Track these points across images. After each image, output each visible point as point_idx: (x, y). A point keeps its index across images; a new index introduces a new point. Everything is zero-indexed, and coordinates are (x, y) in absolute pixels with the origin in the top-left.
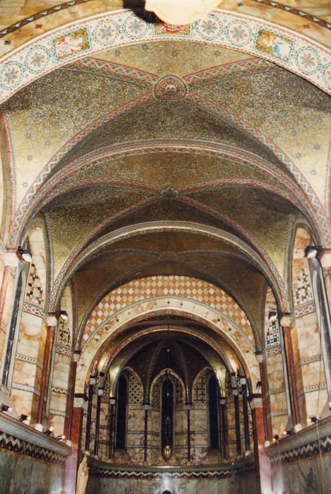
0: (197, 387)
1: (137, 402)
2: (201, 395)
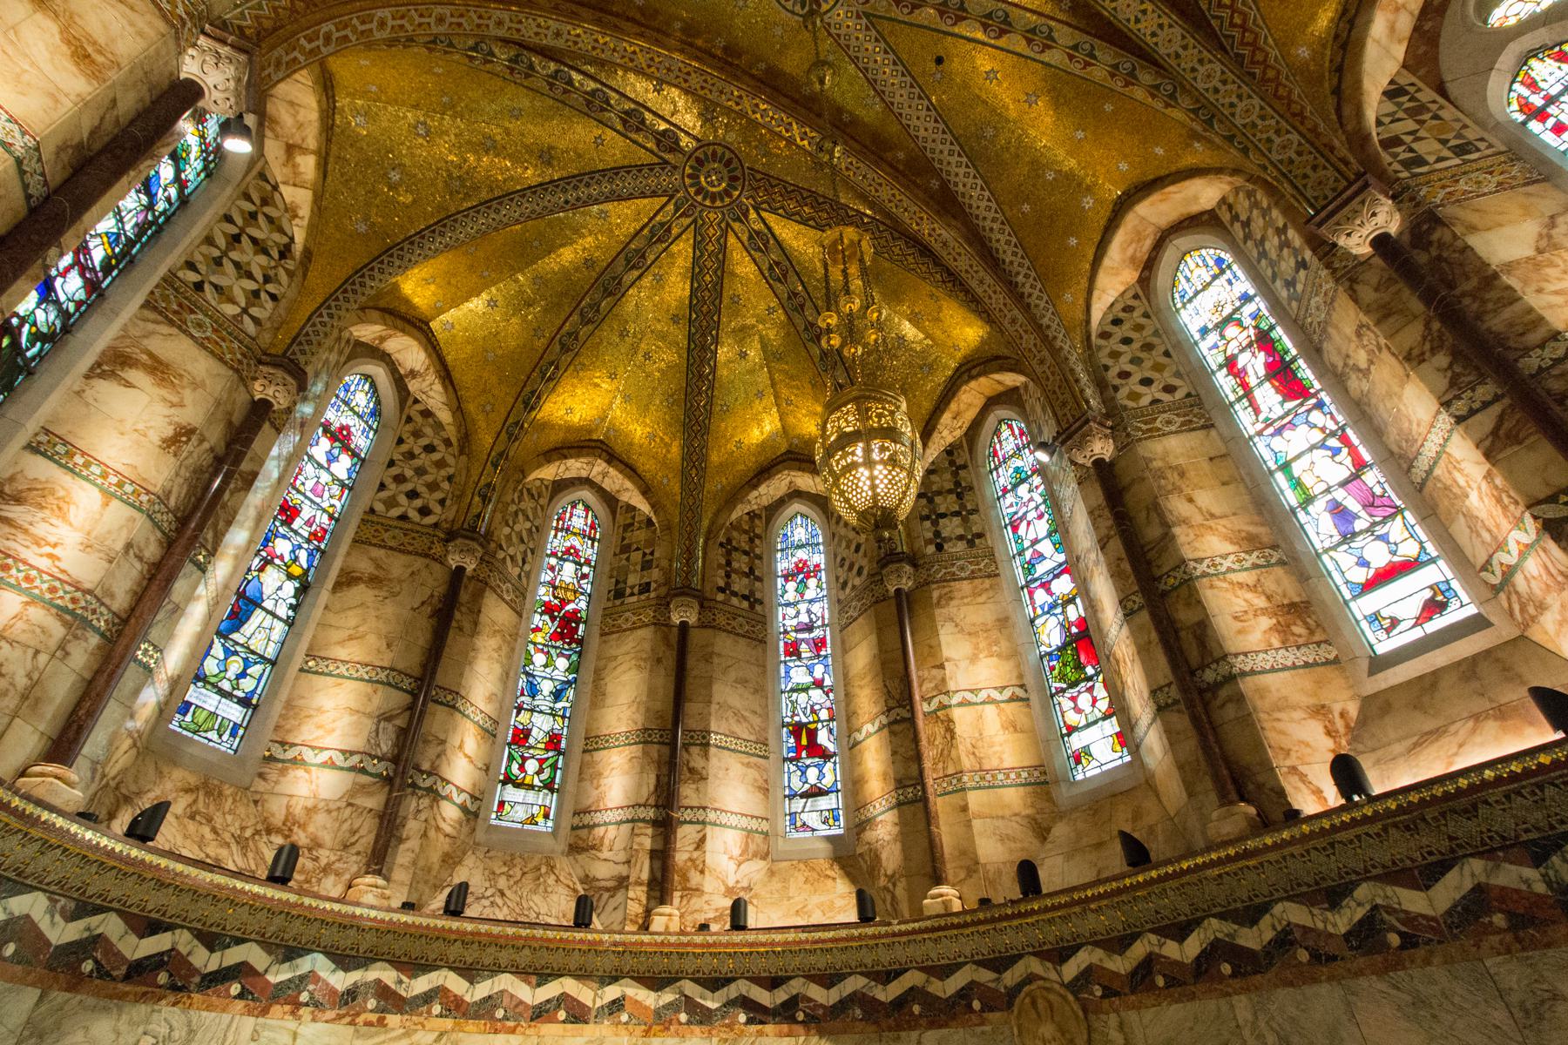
0: (729, 541)
1: (413, 515)
2: (747, 575)
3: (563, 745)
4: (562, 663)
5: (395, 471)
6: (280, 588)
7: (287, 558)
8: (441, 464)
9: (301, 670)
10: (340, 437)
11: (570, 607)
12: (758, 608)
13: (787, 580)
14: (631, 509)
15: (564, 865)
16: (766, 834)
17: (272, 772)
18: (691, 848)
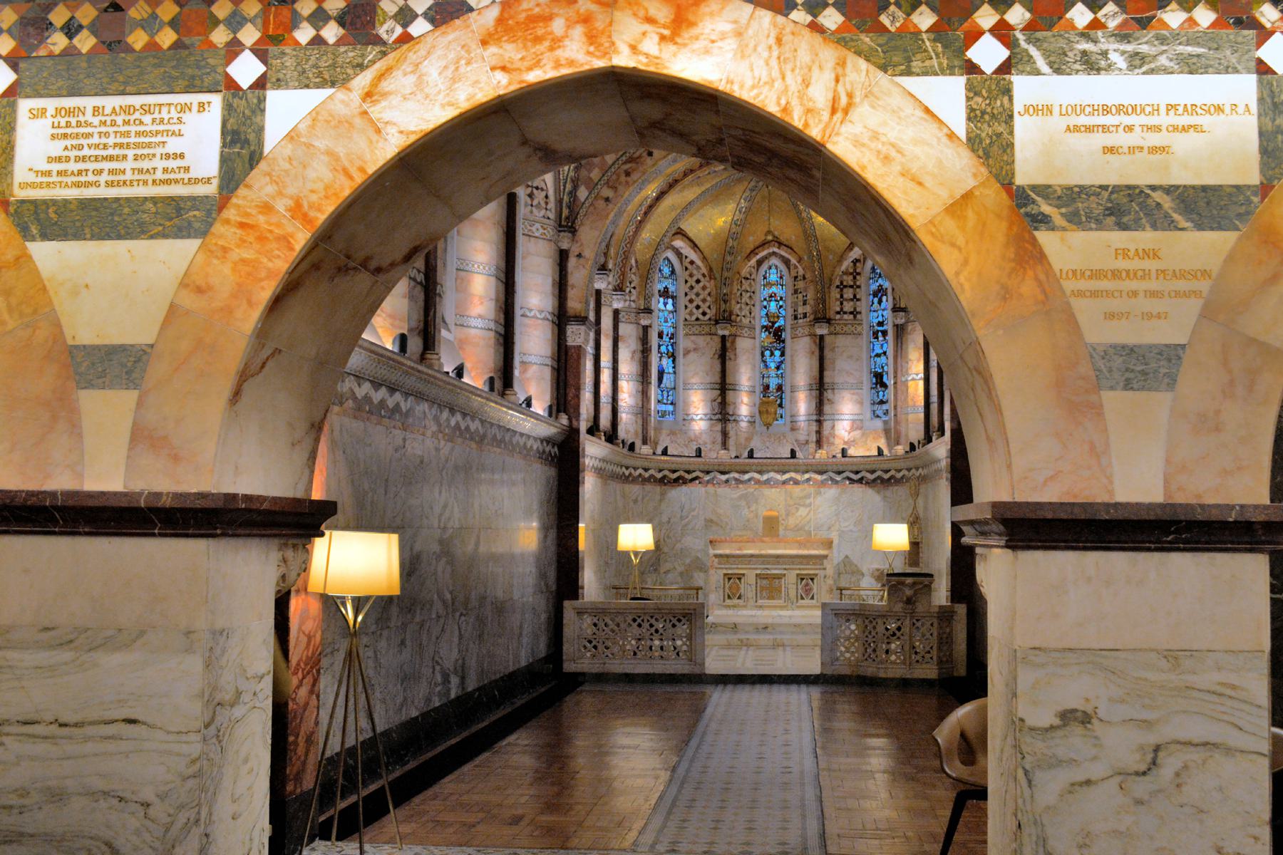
0: (842, 283)
1: (701, 317)
2: (852, 300)
4: (777, 353)
5: (688, 297)
8: (704, 288)
10: (665, 293)
11: (776, 325)
12: (858, 316)
15: (790, 436)
16: (861, 420)
17: (686, 423)
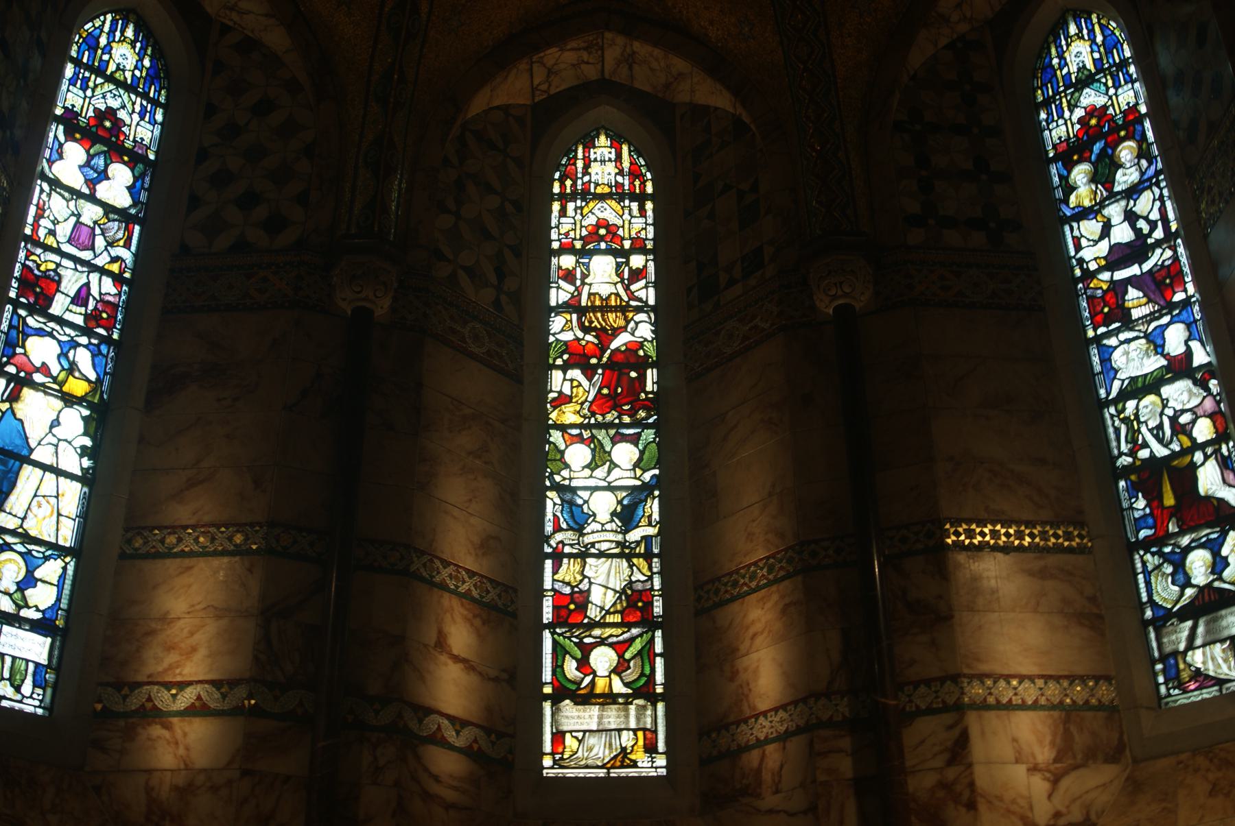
3: (658, 608)
4: (625, 454)
6: (56, 423)
7: (55, 369)
9: (123, 556)
13: (1069, 166)
14: (700, 112)
16: (1110, 710)
18: (939, 762)
